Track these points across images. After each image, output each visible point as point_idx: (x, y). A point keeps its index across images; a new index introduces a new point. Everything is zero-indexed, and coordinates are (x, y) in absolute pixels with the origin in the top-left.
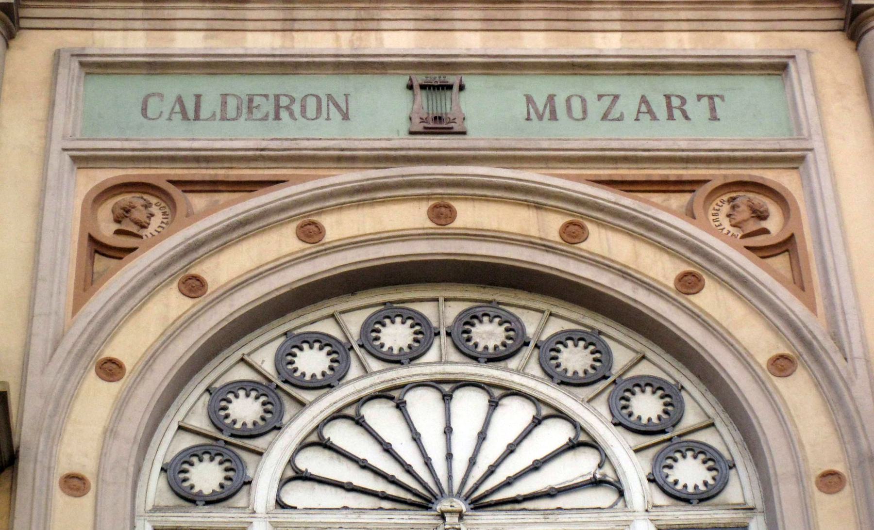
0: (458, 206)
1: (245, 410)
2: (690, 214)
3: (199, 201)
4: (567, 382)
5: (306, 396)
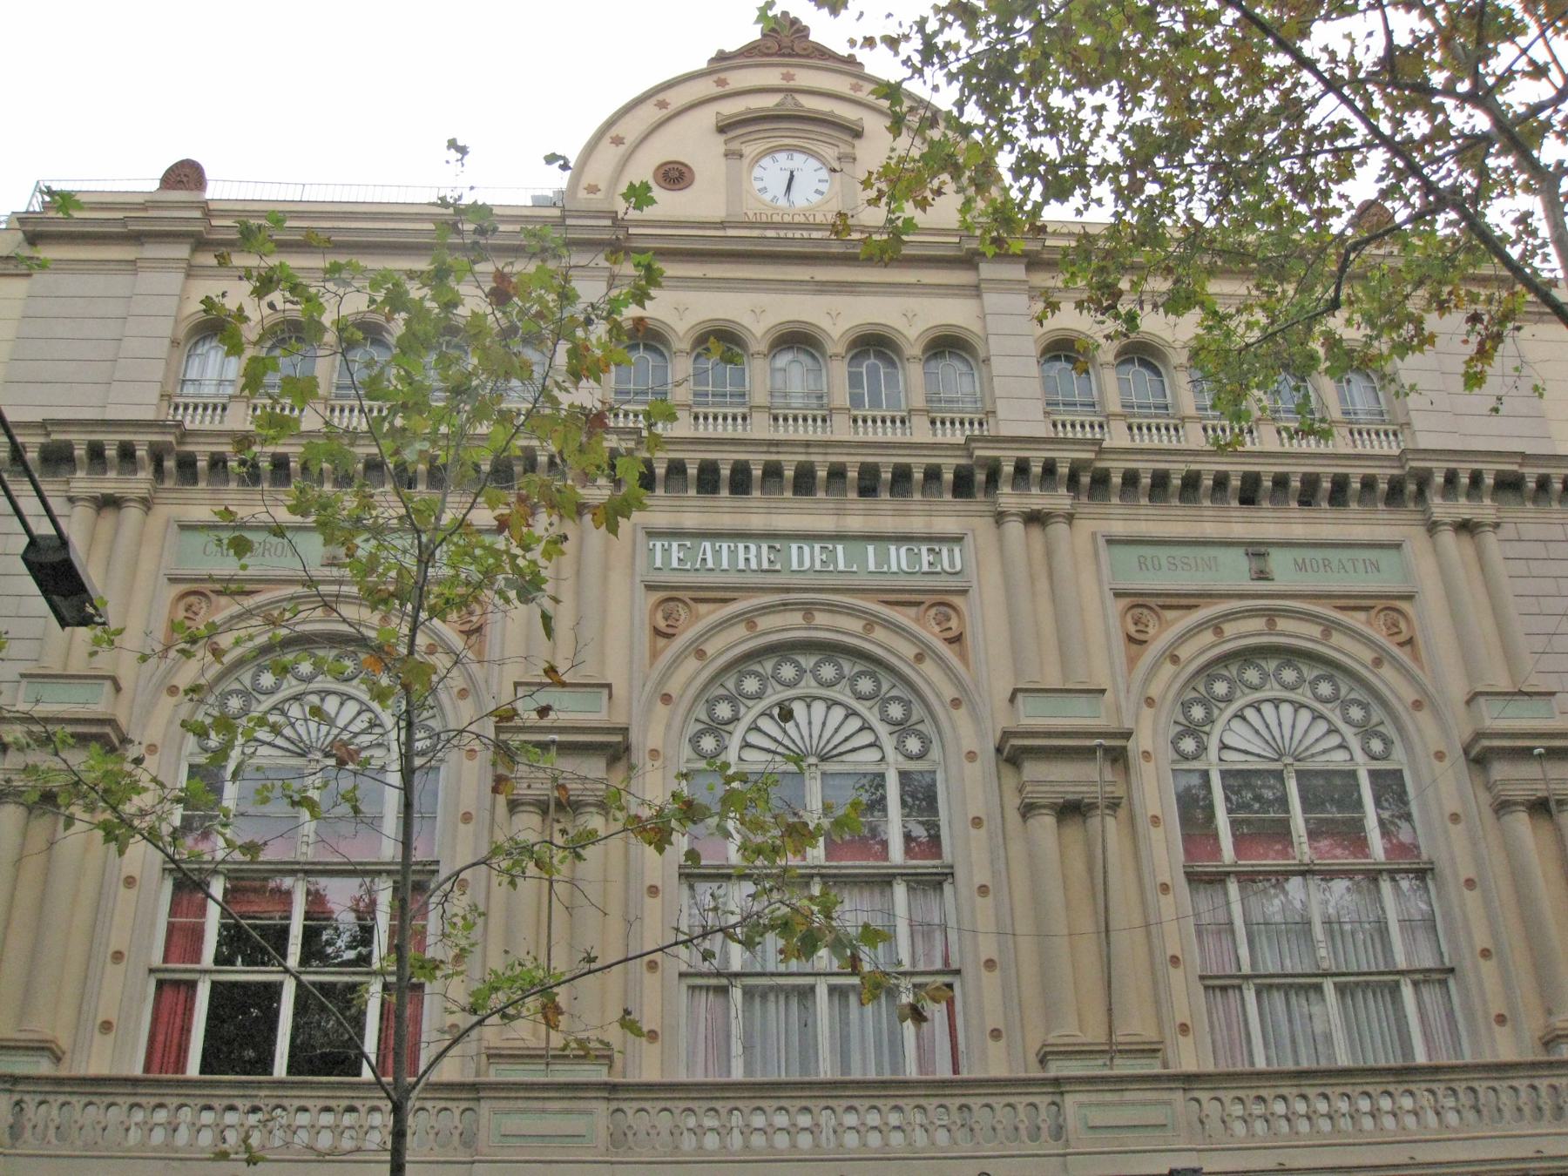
0: (816, 614)
1: (724, 710)
2: (917, 620)
3: (703, 608)
4: (860, 697)
5: (750, 703)
